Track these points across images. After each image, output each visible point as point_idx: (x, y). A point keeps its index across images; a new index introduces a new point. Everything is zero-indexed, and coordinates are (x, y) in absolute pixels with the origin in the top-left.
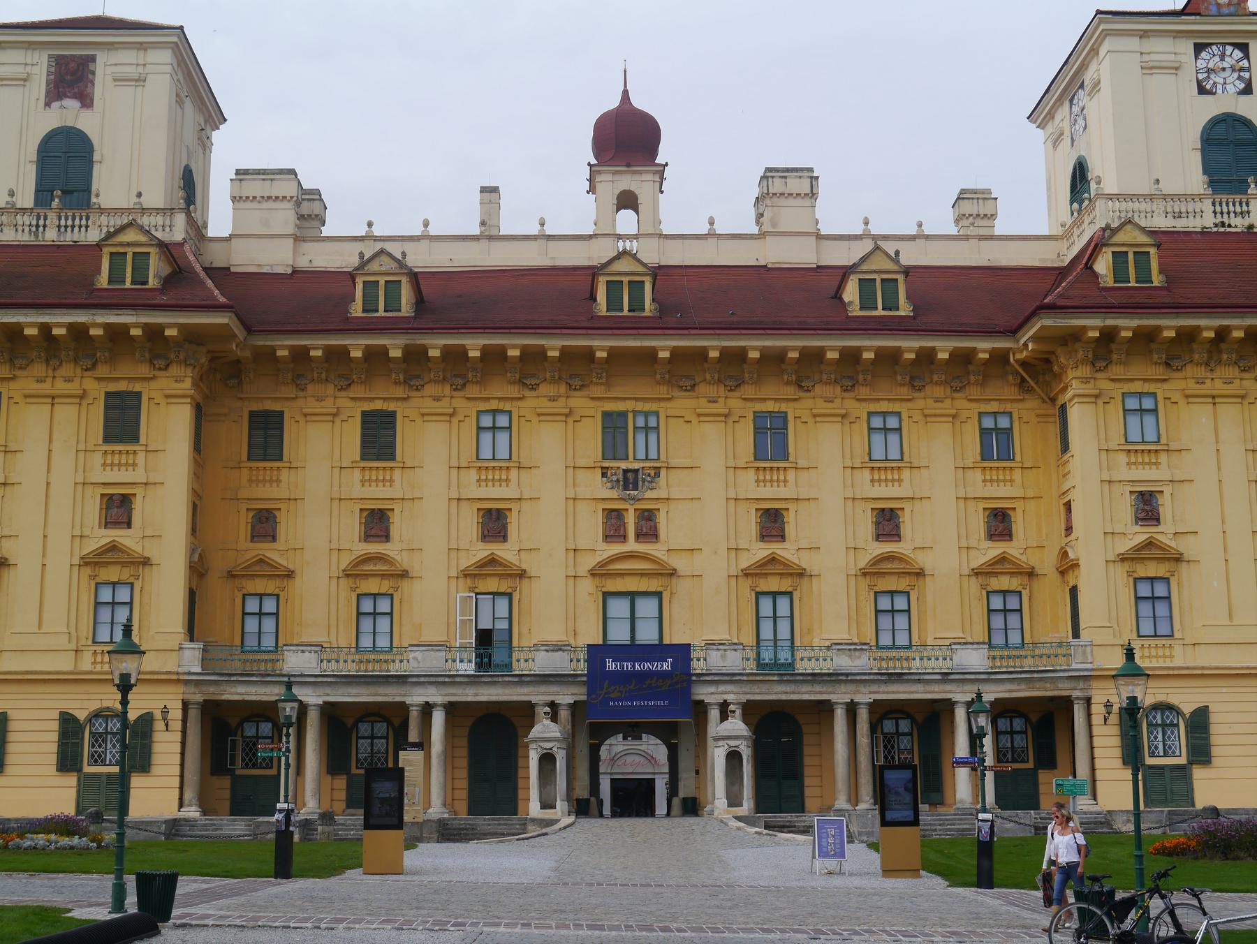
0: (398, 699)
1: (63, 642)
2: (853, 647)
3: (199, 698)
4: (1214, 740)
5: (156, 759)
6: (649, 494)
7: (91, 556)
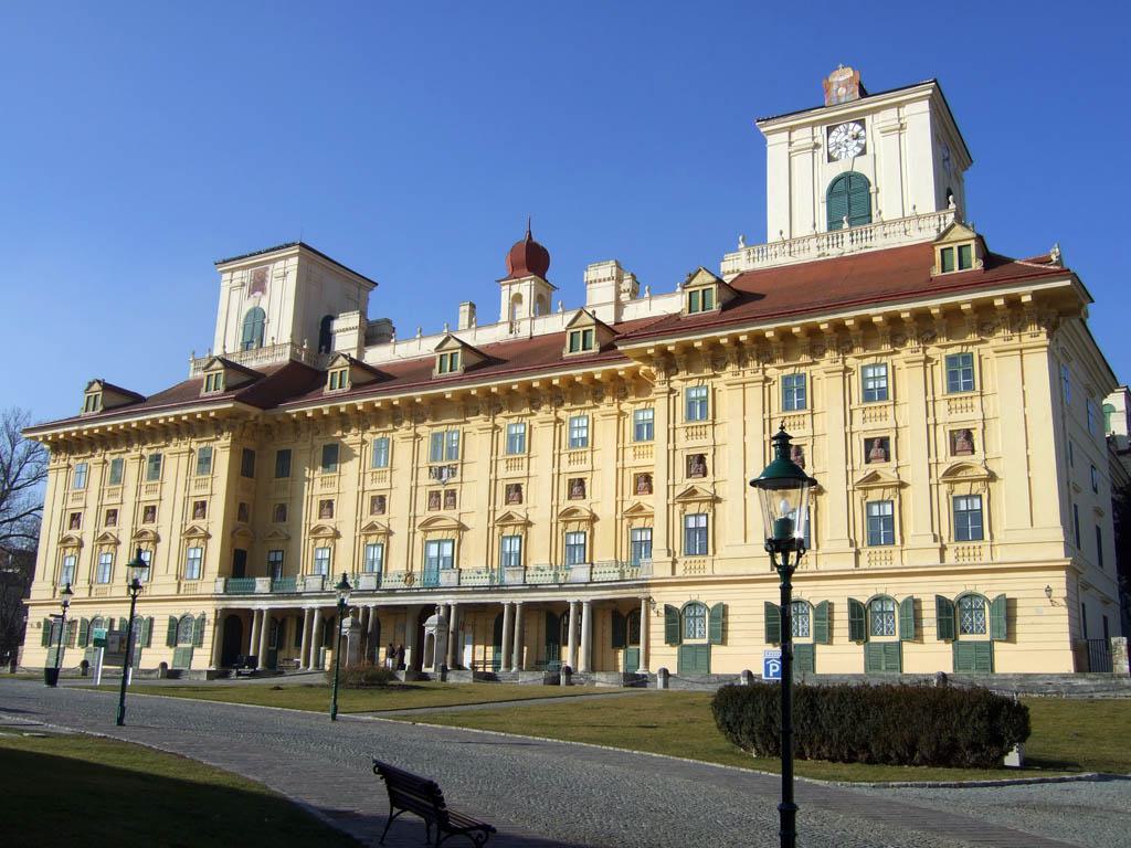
3: (221, 607)
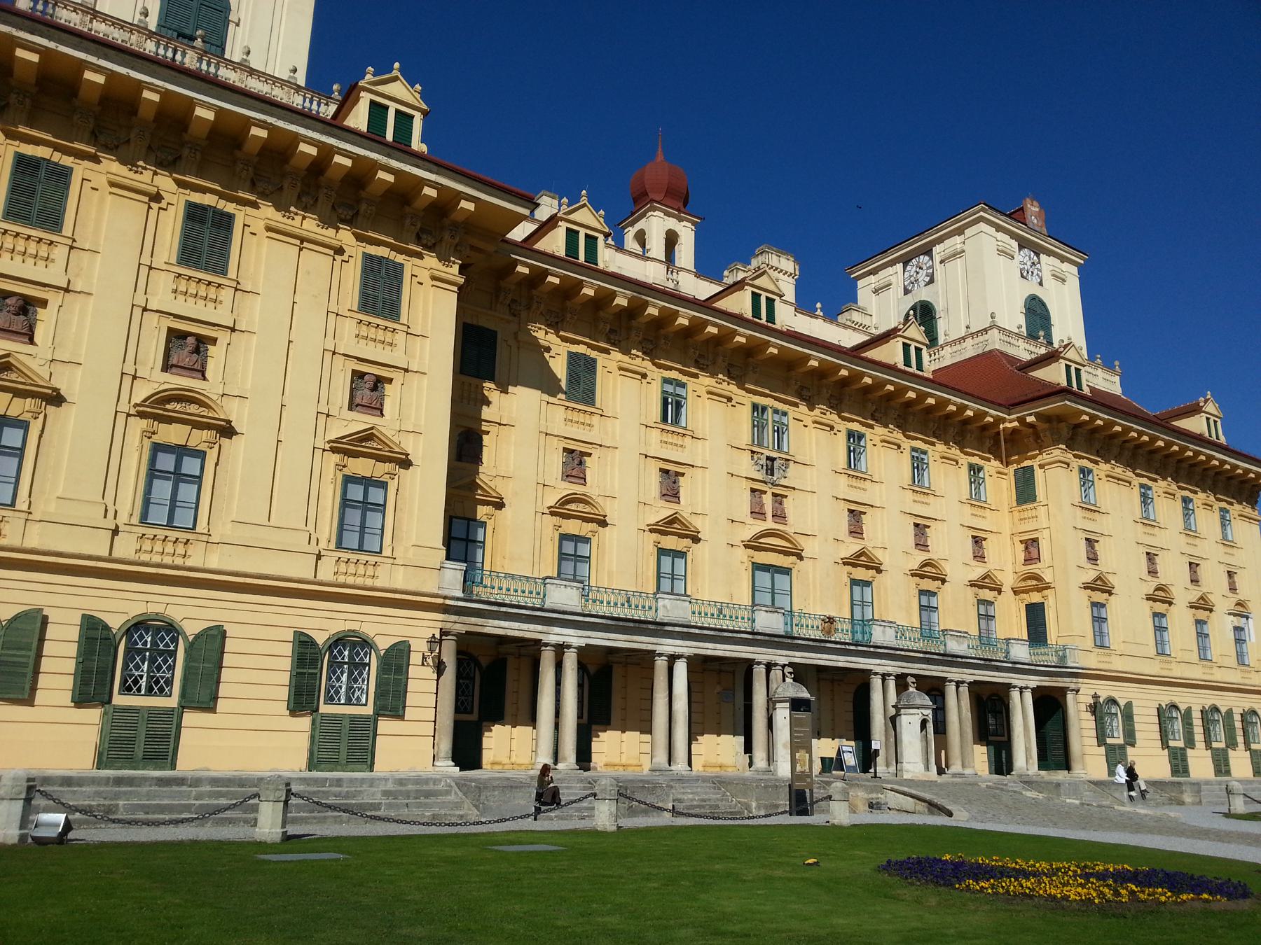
0: (650, 647)
1: (300, 541)
2: (959, 634)
4: (1137, 727)
5: (411, 699)
6: (783, 482)
7: (344, 440)
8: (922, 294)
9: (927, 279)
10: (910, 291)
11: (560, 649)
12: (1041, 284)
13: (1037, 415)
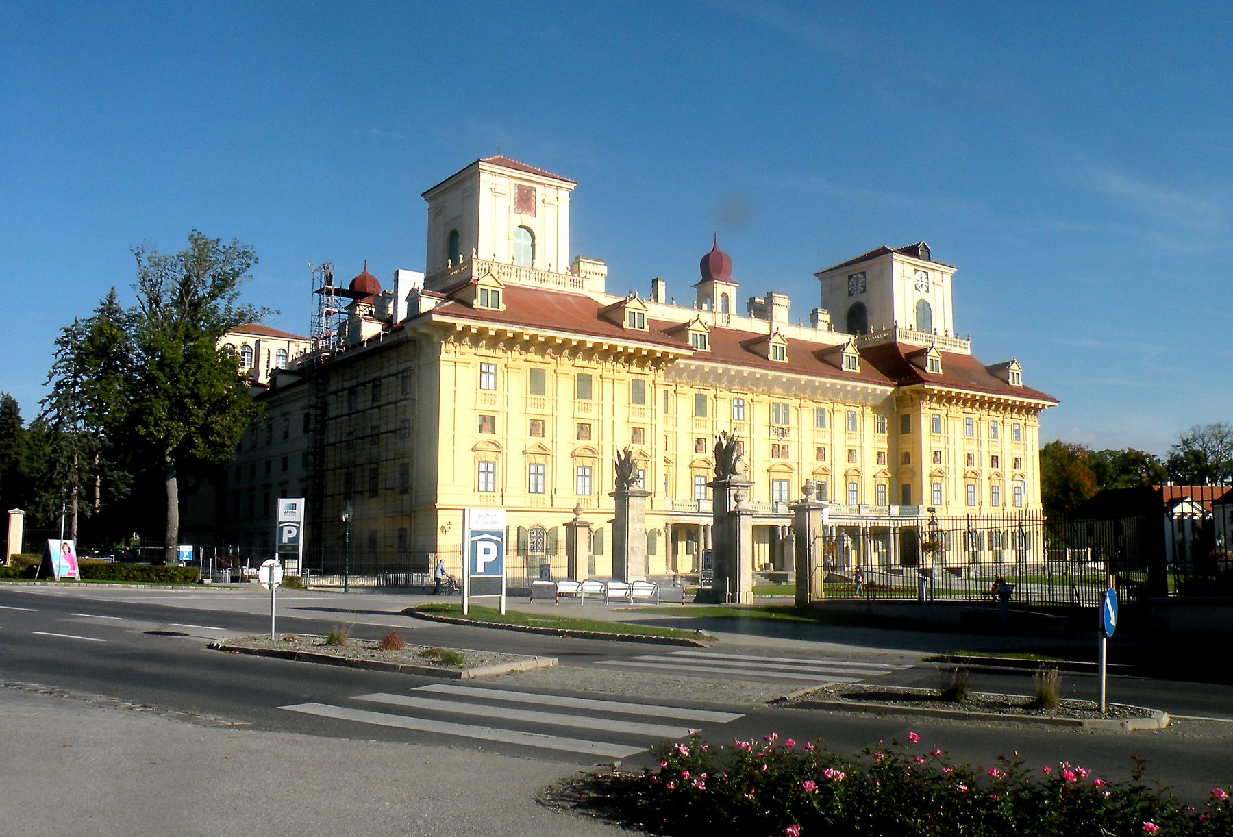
8: (861, 298)
9: (862, 289)
10: (853, 294)
11: (706, 527)
12: (928, 291)
13: (912, 391)
